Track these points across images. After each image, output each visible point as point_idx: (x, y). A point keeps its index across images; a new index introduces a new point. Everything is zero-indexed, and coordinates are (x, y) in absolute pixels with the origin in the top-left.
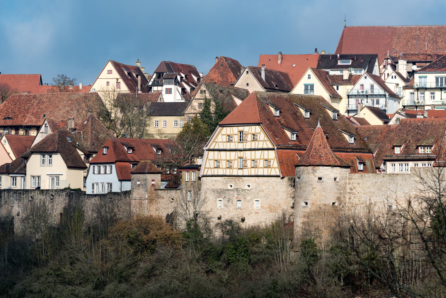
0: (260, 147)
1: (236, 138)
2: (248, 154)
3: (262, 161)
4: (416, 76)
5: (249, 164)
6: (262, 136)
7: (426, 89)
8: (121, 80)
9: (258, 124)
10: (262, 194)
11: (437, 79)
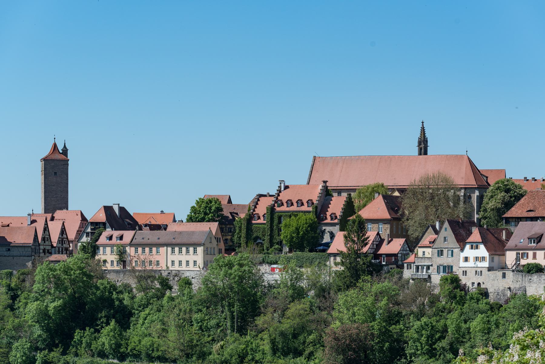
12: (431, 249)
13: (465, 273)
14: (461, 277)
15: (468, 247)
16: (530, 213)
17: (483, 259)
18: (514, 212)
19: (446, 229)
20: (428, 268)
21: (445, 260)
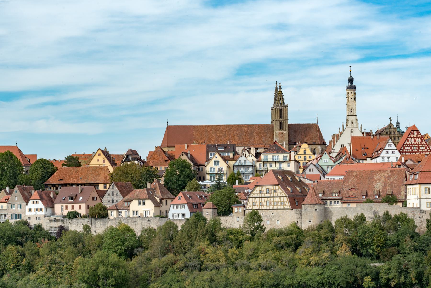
0: (279, 195)
1: (265, 192)
2: (272, 199)
3: (280, 203)
4: (262, 156)
5: (273, 203)
6: (280, 191)
7: (268, 162)
8: (106, 159)
9: (278, 185)
10: (281, 217)
11: (273, 156)
12: (6, 204)
13: (29, 218)
14: (29, 221)
15: (31, 202)
16: (61, 181)
17: (41, 210)
18: (52, 180)
19: (16, 192)
20: (5, 215)
21: (16, 210)
